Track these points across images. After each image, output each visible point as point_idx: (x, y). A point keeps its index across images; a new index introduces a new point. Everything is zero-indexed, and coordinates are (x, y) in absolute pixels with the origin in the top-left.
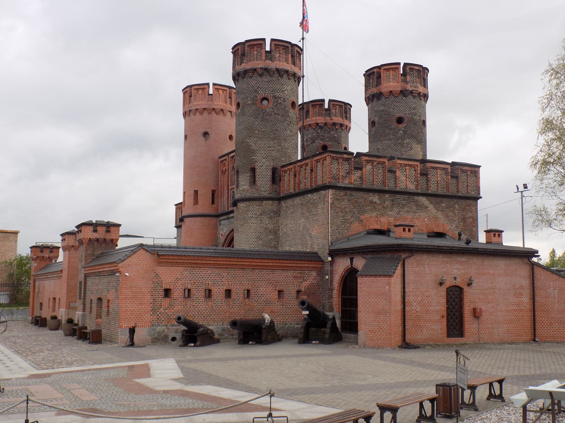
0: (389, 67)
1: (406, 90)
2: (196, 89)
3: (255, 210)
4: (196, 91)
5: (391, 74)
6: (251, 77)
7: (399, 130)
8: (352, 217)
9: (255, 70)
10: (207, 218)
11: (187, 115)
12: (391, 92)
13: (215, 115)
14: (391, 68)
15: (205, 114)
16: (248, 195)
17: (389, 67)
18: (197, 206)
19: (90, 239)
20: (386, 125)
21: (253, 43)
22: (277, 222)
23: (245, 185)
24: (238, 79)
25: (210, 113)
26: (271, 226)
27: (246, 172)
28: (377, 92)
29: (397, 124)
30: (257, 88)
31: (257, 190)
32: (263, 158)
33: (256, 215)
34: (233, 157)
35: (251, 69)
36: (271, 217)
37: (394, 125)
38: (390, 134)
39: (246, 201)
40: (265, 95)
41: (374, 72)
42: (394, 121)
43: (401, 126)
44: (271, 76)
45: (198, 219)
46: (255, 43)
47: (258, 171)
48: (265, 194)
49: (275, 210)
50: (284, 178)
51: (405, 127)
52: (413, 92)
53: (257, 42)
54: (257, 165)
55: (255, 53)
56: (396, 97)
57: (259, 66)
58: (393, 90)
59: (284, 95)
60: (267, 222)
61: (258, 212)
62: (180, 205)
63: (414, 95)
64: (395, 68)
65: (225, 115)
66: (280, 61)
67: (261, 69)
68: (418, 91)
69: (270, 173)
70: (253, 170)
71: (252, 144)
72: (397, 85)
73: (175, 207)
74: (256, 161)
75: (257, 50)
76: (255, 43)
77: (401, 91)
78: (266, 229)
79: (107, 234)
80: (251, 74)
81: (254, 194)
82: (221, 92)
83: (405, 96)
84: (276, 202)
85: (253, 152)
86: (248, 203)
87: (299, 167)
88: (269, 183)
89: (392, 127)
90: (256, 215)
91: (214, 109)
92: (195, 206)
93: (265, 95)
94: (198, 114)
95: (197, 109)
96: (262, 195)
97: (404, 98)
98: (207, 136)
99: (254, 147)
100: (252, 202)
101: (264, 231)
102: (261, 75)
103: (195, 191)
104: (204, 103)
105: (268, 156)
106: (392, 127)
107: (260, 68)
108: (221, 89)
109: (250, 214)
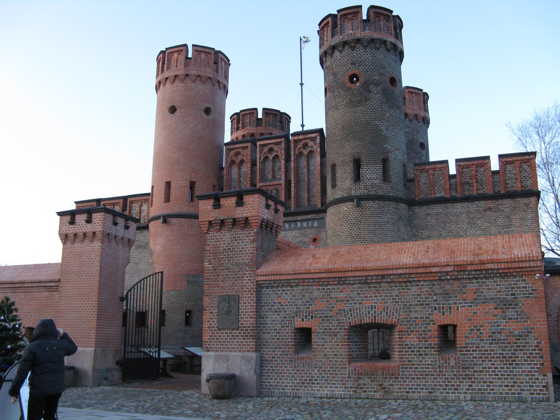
3: (391, 214)
4: (197, 53)
9: (385, 42)
11: (177, 80)
12: (416, 115)
14: (415, 93)
16: (381, 193)
27: (377, 163)
29: (420, 149)
33: (393, 219)
35: (380, 40)
39: (379, 200)
42: (418, 145)
46: (382, 11)
54: (391, 156)
57: (390, 40)
67: (392, 43)
70: (385, 162)
71: (383, 128)
73: (75, 205)
74: (389, 151)
76: (382, 11)
80: (378, 46)
82: (223, 63)
85: (386, 138)
89: (417, 151)
91: (219, 82)
99: (385, 132)
102: (388, 51)
107: (391, 42)
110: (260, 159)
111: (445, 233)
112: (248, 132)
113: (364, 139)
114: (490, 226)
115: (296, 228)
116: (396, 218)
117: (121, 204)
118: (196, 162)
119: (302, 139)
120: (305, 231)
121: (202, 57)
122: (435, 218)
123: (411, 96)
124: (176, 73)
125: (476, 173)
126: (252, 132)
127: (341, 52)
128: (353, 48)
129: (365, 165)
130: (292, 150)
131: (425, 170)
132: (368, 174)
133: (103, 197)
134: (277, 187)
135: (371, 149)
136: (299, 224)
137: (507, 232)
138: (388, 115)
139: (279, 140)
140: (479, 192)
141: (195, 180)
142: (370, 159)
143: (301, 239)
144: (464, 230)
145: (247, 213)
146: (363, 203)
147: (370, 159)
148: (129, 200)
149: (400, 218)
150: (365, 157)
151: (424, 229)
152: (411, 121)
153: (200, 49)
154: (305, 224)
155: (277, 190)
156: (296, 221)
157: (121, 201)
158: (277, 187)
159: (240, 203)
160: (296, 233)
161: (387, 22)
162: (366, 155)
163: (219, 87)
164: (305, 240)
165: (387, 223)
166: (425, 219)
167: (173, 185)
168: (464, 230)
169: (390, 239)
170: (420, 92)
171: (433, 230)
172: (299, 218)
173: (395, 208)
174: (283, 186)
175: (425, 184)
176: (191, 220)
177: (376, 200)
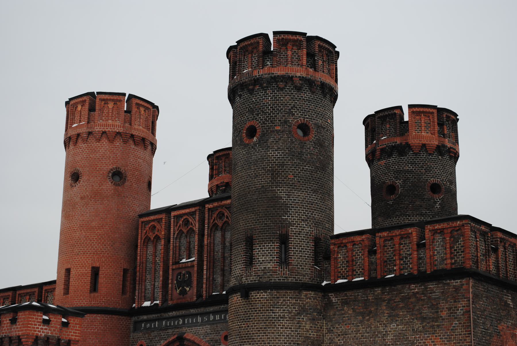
0: (421, 109)
1: (444, 146)
2: (104, 100)
3: (288, 306)
4: (103, 102)
5: (423, 120)
6: (282, 89)
7: (435, 203)
8: (491, 325)
9: (291, 78)
10: (114, 316)
11: (80, 140)
12: (424, 145)
13: (133, 147)
14: (423, 112)
15: (118, 143)
16: (275, 279)
17: (421, 109)
18: (96, 294)
19: (37, 337)
20: (416, 192)
21: (286, 37)
22: (321, 328)
23: (270, 263)
24: (253, 90)
25: (125, 142)
26: (313, 334)
27: (272, 241)
28: (401, 144)
29: (432, 194)
30: (292, 108)
31: (292, 271)
32: (302, 220)
34: (178, 217)
35: (283, 77)
36: (314, 319)
37: (428, 194)
38: (421, 206)
39: (272, 290)
40: (304, 120)
41: (395, 114)
43: (438, 198)
44: (313, 93)
45: (99, 317)
47: (293, 241)
48: (306, 279)
49: (319, 307)
50: (337, 255)
51: (442, 199)
52: (451, 150)
53: (294, 37)
54: (293, 230)
55: (289, 53)
56: (430, 154)
57: (298, 74)
58: (427, 143)
59: (327, 125)
60: (308, 327)
61: (294, 308)
62: (10, 293)
63: (451, 154)
64: (429, 113)
65: (145, 148)
66: (323, 71)
67: (301, 78)
68: (455, 150)
69: (312, 244)
71: (283, 195)
72: (433, 137)
74: (290, 223)
75: (292, 49)
77: (438, 147)
78: (307, 338)
79: (65, 329)
80: (281, 85)
81: (286, 277)
82: (142, 109)
83: (441, 154)
84: (320, 294)
86: (275, 292)
87: (382, 240)
88: (311, 262)
89: (426, 197)
90: (290, 313)
91: (132, 136)
92: (92, 295)
93: (304, 120)
94: (105, 142)
95: (104, 133)
96: (300, 280)
97: (440, 157)
98: (117, 178)
100: (283, 292)
101: (304, 341)
102: (299, 89)
103: (93, 268)
104: (118, 123)
105: (309, 218)
106: (426, 197)
107: (299, 77)
108: (143, 106)
109: (279, 312)
110: (174, 234)
111: (363, 328)
112: (222, 181)
113: (258, 210)
114: (413, 319)
115: (209, 322)
116: (296, 311)
117: (36, 294)
118: (99, 243)
119: (217, 207)
120: (217, 327)
121: (110, 107)
122: (352, 309)
123: (418, 117)
124: (79, 131)
125: (399, 247)
126: (226, 181)
127: (240, 96)
128: (251, 92)
129: (258, 244)
130: (206, 221)
131: (342, 245)
132: (260, 256)
133: (23, 284)
134: (190, 270)
135: (265, 224)
136: (212, 317)
137: (432, 327)
138: (291, 176)
139: (193, 209)
140: (435, 268)
141: (97, 265)
142: (264, 236)
143: (212, 336)
144: (384, 324)
145: (19, 331)
146: (253, 294)
147: (264, 236)
148: (45, 288)
149: (303, 311)
150: (258, 234)
151: (340, 323)
152: (416, 154)
153: (106, 97)
154: (217, 317)
155: (190, 274)
156: (208, 314)
157: (36, 290)
158: (190, 270)
159: (14, 321)
160: (207, 328)
161: (298, 49)
162: (259, 232)
163: (135, 142)
164: (217, 338)
165: (281, 318)
166: (341, 310)
167: (73, 272)
168: (384, 324)
169: (285, 338)
170: (431, 110)
171: (350, 324)
172: (211, 309)
173: (295, 298)
174: (196, 269)
175: (343, 262)
176: (92, 315)
177: (268, 289)
